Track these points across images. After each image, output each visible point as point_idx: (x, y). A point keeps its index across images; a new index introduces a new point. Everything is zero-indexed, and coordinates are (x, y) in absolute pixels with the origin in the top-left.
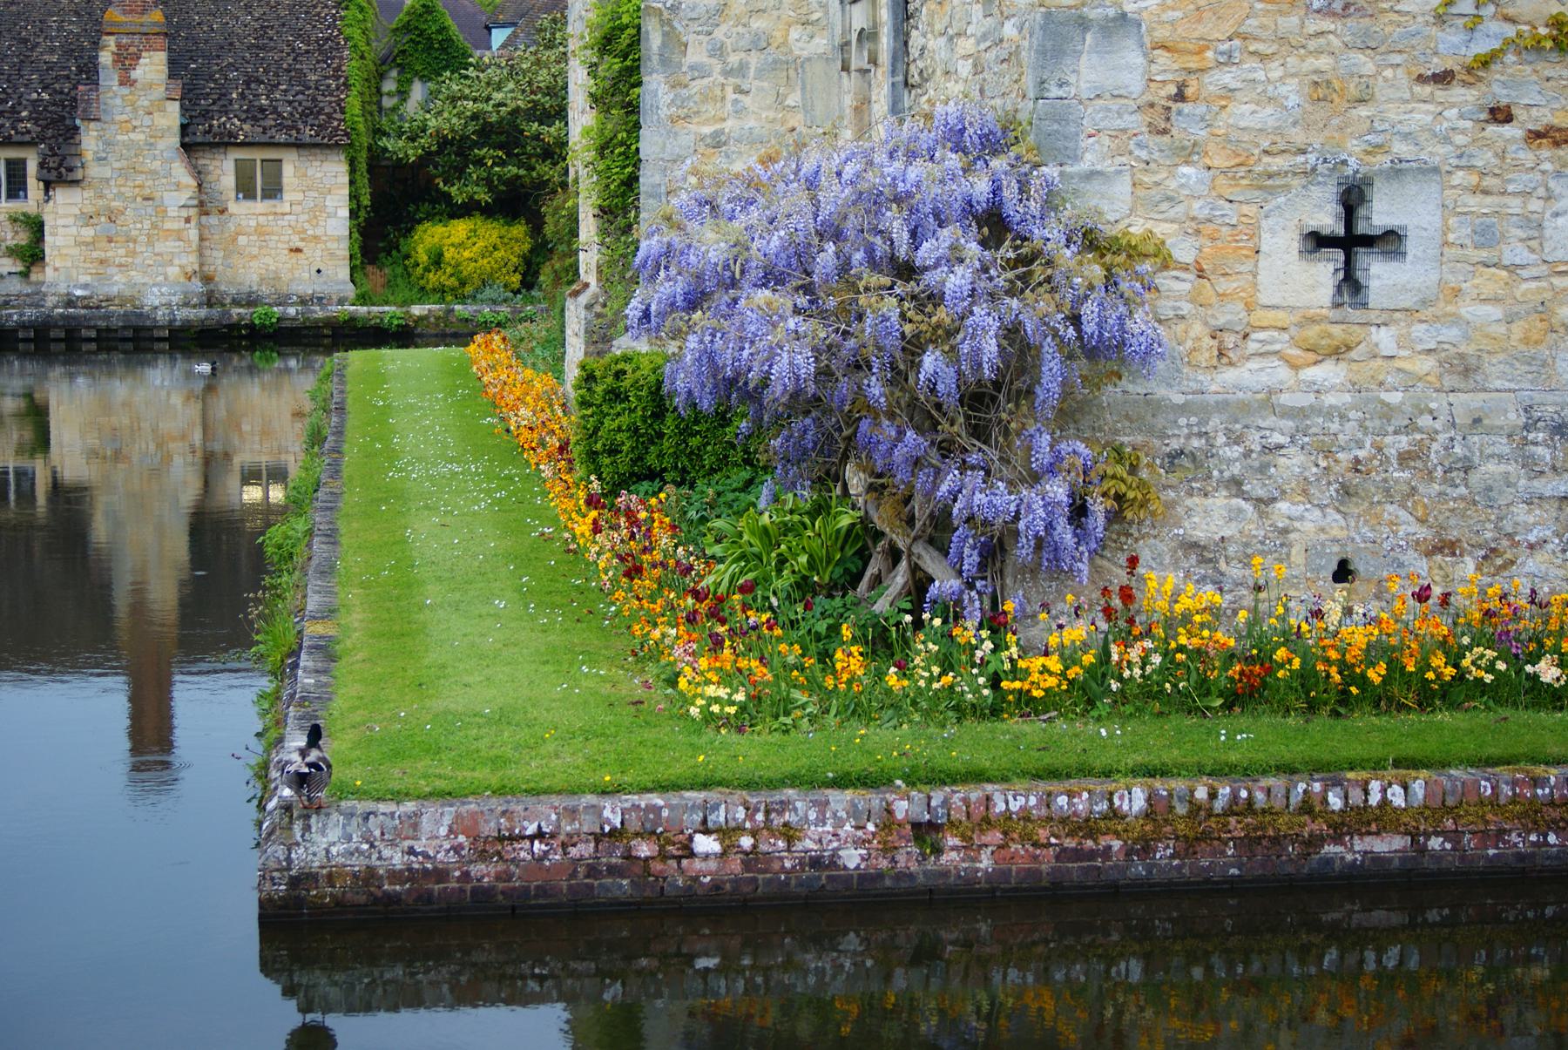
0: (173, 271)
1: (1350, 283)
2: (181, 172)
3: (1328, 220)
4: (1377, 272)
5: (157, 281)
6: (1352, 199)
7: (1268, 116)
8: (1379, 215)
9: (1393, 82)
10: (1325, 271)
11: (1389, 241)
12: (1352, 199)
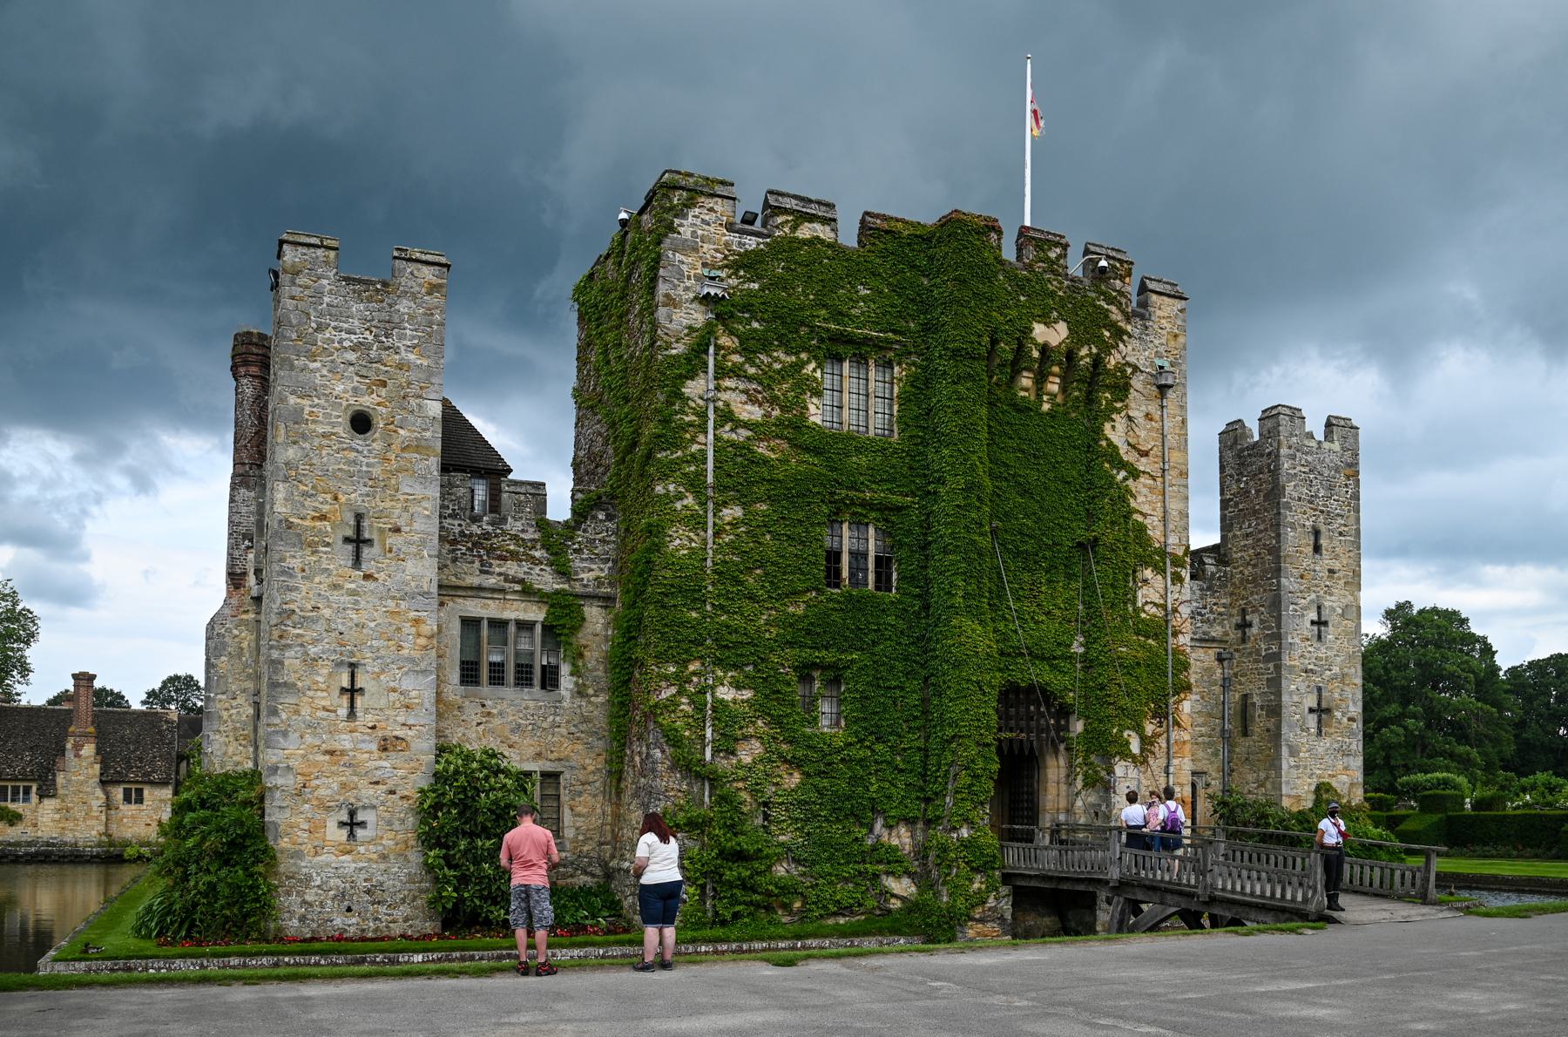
0: (94, 833)
1: (352, 835)
2: (99, 793)
3: (345, 818)
4: (359, 832)
5: (86, 832)
6: (352, 814)
7: (329, 792)
8: (360, 817)
9: (363, 783)
10: (344, 832)
11: (362, 824)
12: (352, 814)
